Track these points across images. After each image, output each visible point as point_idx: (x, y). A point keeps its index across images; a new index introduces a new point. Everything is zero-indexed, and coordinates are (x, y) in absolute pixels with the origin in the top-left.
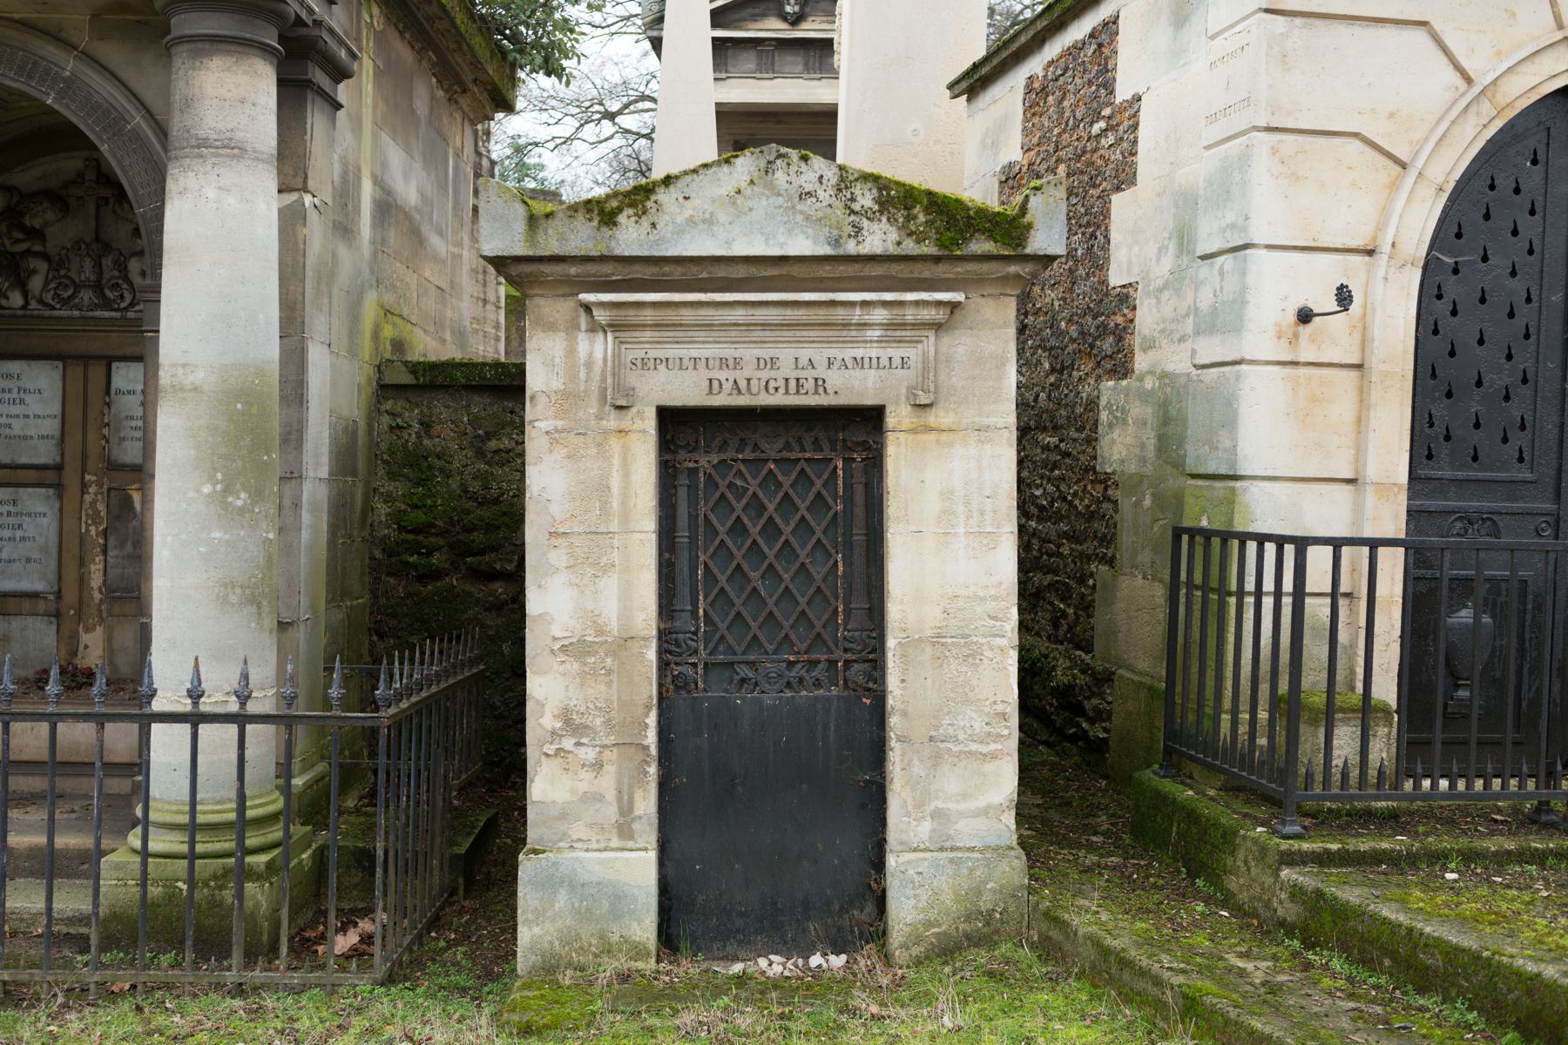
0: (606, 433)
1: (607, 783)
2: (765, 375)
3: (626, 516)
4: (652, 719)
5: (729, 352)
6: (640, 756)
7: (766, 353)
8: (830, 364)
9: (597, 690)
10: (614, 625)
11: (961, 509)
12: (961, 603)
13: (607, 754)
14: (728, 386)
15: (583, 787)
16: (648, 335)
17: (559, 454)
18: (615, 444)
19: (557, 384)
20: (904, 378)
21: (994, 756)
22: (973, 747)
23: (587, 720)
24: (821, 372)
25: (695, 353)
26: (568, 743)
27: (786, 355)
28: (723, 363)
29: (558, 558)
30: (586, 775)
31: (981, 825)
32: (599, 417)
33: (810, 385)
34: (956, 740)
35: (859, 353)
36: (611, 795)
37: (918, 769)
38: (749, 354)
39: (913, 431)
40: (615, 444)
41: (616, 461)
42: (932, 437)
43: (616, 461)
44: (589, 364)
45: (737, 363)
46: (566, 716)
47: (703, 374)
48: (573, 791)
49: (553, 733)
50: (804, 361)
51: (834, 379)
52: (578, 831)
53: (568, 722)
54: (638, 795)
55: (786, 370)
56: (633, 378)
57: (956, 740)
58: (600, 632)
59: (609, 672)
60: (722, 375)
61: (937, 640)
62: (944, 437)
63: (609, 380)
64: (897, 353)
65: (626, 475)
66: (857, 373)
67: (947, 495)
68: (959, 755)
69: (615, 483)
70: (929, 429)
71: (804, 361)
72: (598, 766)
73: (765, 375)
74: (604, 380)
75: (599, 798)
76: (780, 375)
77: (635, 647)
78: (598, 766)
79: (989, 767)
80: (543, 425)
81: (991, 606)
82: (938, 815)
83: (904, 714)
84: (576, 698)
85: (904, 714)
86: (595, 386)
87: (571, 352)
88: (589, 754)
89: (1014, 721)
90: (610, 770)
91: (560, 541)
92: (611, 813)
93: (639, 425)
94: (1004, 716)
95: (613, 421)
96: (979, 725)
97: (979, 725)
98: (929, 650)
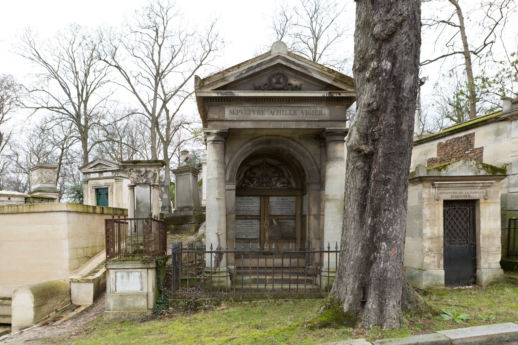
0: (435, 204)
1: (436, 259)
2: (460, 194)
3: (438, 217)
4: (443, 249)
5: (455, 191)
6: (441, 255)
7: (461, 191)
8: (471, 193)
9: (434, 245)
10: (437, 234)
11: (492, 215)
12: (492, 230)
13: (436, 255)
14: (455, 196)
15: (432, 260)
16: (443, 188)
17: (428, 207)
18: (437, 206)
19: (427, 196)
20: (483, 195)
21: (497, 254)
22: (494, 252)
23: (433, 249)
24: (470, 194)
25: (449, 191)
26: (430, 253)
27: (464, 191)
28: (454, 193)
29: (428, 224)
30: (433, 258)
31: (495, 265)
32: (434, 202)
33: (468, 196)
34: (491, 251)
35: (476, 191)
36: (436, 261)
37: (485, 256)
38: (458, 191)
39: (484, 203)
40: (437, 206)
41: (437, 209)
42: (487, 204)
43: (437, 209)
44: (432, 193)
45: (456, 193)
46: (429, 249)
47: (451, 195)
48: (430, 261)
49: (427, 252)
50: (467, 192)
51: (472, 195)
52: (431, 267)
53: (430, 250)
54: (441, 261)
55: (464, 194)
56: (439, 195)
57: (491, 251)
58: (435, 236)
59: (436, 242)
60: (454, 195)
61: (488, 236)
62: (489, 204)
63: (436, 196)
64: (481, 191)
65: (438, 211)
66: (475, 194)
67: (490, 213)
68: (492, 254)
69: (437, 212)
70: (487, 203)
71: (467, 192)
72: (434, 257)
73: (460, 194)
74: (435, 196)
75: (434, 262)
76: (463, 194)
77: (440, 238)
78: (434, 257)
79: (497, 256)
80: (425, 203)
81: (497, 230)
82: (489, 263)
83: (483, 248)
84: (431, 246)
85: (483, 248)
86: (433, 197)
87: (429, 191)
88: (433, 255)
89: (501, 248)
90: (436, 257)
91: (428, 221)
92: (436, 264)
93: (440, 203)
94: (499, 248)
95: (436, 202)
96: (495, 249)
97: (495, 249)
98: (487, 238)
